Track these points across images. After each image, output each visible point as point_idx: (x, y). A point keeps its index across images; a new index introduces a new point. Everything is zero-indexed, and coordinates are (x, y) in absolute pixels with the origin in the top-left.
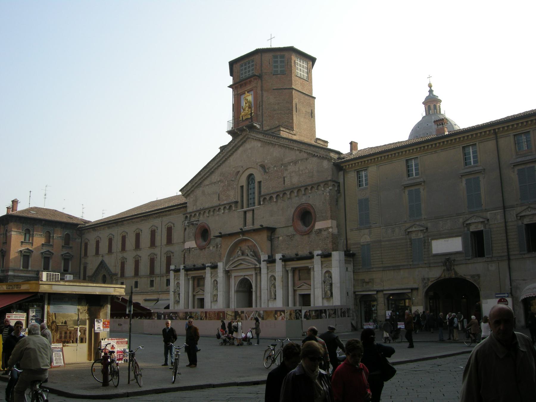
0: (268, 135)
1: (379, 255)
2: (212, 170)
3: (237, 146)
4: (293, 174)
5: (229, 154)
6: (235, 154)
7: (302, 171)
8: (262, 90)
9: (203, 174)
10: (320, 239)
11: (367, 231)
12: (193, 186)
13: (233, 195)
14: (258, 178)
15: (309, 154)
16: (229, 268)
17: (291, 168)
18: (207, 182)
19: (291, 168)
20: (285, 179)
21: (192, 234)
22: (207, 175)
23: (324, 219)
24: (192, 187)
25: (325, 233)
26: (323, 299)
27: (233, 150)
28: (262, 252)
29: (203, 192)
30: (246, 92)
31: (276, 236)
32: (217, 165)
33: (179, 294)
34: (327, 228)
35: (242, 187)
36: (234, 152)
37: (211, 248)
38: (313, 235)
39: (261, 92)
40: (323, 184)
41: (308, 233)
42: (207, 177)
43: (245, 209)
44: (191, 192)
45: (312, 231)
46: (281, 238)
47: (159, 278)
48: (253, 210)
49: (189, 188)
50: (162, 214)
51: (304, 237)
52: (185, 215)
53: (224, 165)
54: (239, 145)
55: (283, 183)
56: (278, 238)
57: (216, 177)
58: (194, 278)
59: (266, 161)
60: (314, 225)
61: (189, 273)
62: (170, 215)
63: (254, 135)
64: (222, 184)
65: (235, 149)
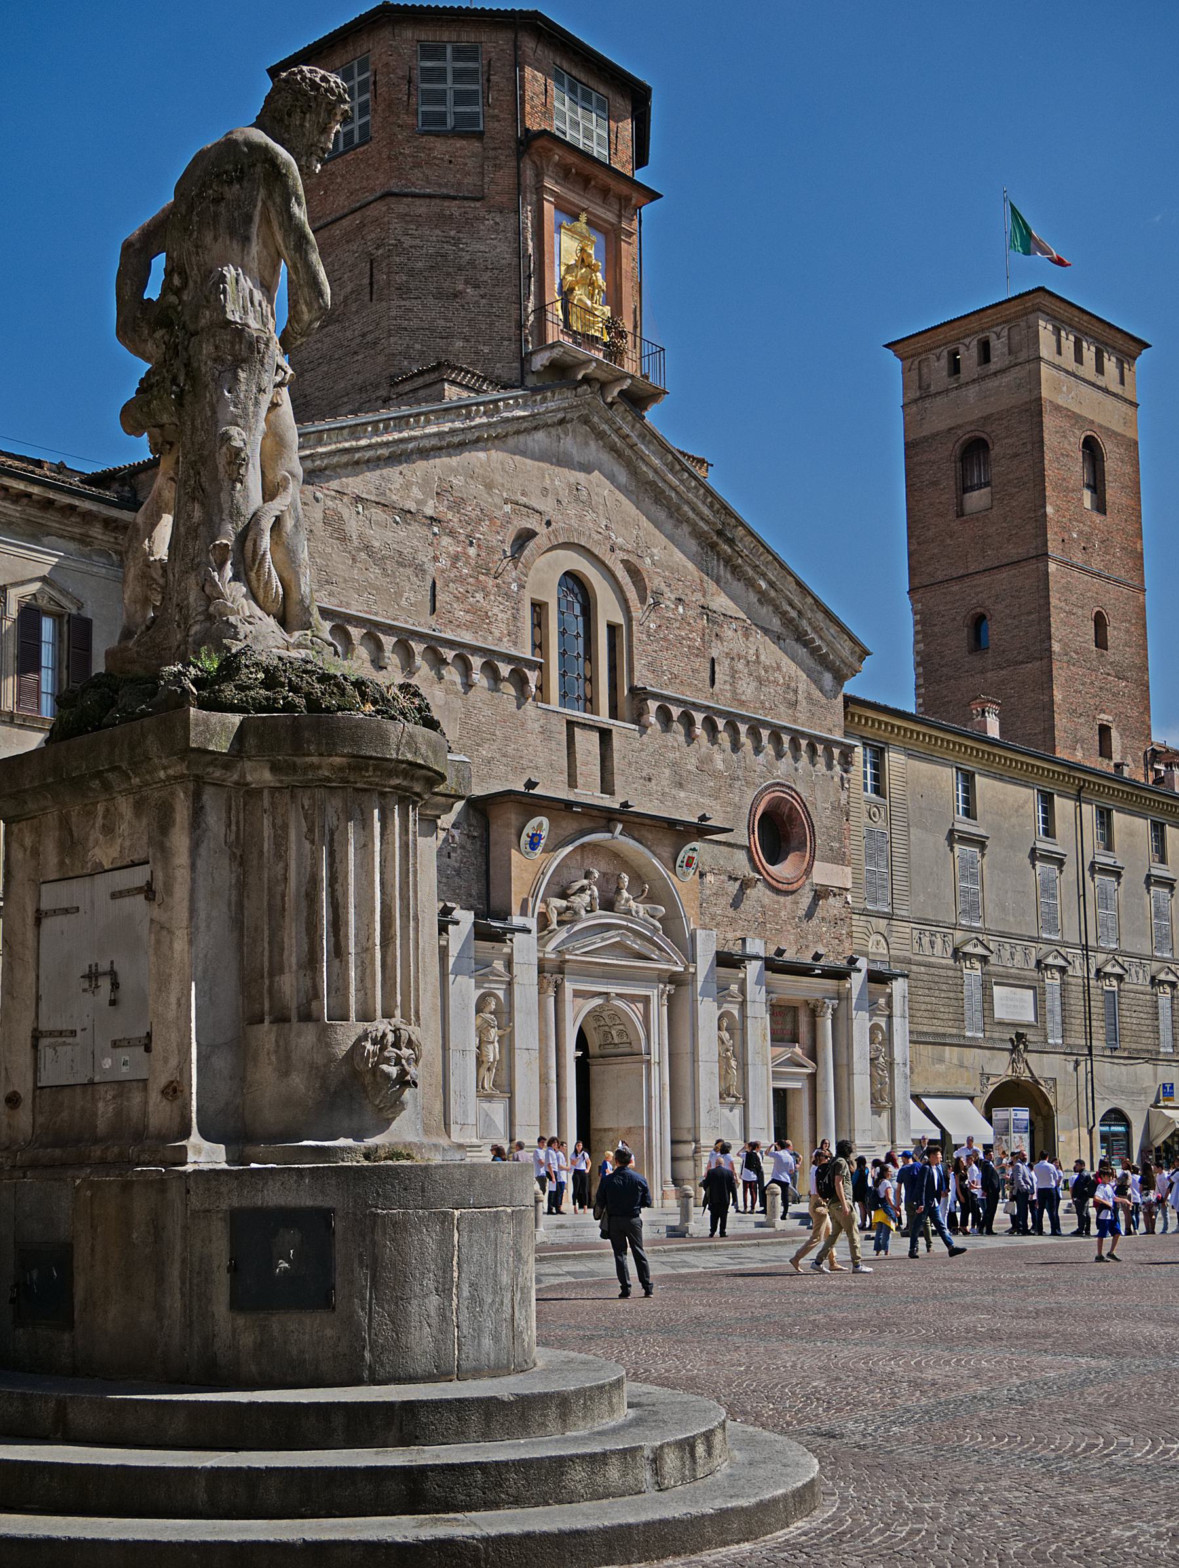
15: (788, 622)
18: (355, 484)
23: (839, 858)
30: (583, 217)
45: (804, 884)
46: (710, 878)
48: (605, 735)
55: (706, 675)
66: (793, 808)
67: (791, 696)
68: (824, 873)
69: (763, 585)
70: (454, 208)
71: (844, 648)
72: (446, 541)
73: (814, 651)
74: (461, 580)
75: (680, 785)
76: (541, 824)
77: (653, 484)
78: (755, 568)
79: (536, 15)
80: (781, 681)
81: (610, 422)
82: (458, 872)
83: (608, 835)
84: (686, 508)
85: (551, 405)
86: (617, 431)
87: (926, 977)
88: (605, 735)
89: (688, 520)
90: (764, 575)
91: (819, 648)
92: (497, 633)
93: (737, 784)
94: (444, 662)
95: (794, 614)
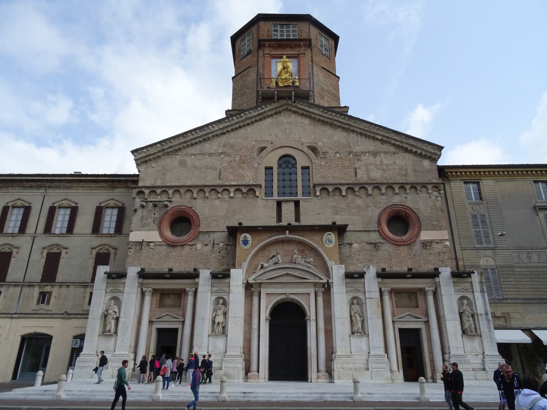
0: (333, 112)
1: (513, 283)
2: (210, 136)
3: (265, 115)
4: (372, 167)
5: (249, 121)
6: (256, 124)
7: (387, 166)
8: (312, 62)
9: (192, 137)
10: (430, 254)
11: (489, 253)
12: (164, 150)
13: (253, 175)
14: (301, 161)
15: (398, 147)
16: (253, 280)
17: (367, 159)
18: (191, 150)
19: (367, 159)
20: (358, 170)
21: (151, 221)
22: (197, 140)
24: (159, 152)
25: (437, 248)
26: (462, 336)
27: (258, 118)
28: (330, 260)
29: (183, 164)
30: (285, 57)
31: (345, 242)
32: (221, 131)
33: (117, 319)
34: (441, 241)
35: (269, 169)
36: (256, 121)
37: (199, 246)
38: (417, 247)
39: (310, 63)
40: (432, 185)
41: (409, 244)
42: (196, 143)
43: (276, 197)
44: (154, 158)
45: (415, 241)
46: (355, 245)
47: (18, 289)
48: (297, 204)
49: (152, 151)
50: (48, 184)
51: (402, 248)
52: (138, 190)
53: (232, 134)
54: (269, 113)
56: (351, 244)
57: (215, 147)
58: (155, 291)
59: (320, 144)
60: (418, 235)
61: (147, 281)
62: (70, 188)
63: (302, 107)
64: (228, 159)
65: (261, 117)
66: (406, 213)
67: (403, 172)
68: (425, 235)
69: (380, 137)
70: (245, 73)
71: (430, 149)
72: (226, 158)
73: (415, 153)
74: (232, 167)
75: (337, 214)
76: (245, 236)
77: (319, 120)
78: (373, 133)
79: (259, 15)
80: (397, 168)
81: (296, 107)
82: (224, 257)
83: (284, 236)
84: (335, 123)
85: (266, 109)
86: (300, 108)
87: (527, 273)
88: (297, 204)
89: (340, 127)
90: (379, 135)
91: (416, 152)
92: (247, 180)
93: (370, 209)
94: (218, 192)
95: (397, 143)
